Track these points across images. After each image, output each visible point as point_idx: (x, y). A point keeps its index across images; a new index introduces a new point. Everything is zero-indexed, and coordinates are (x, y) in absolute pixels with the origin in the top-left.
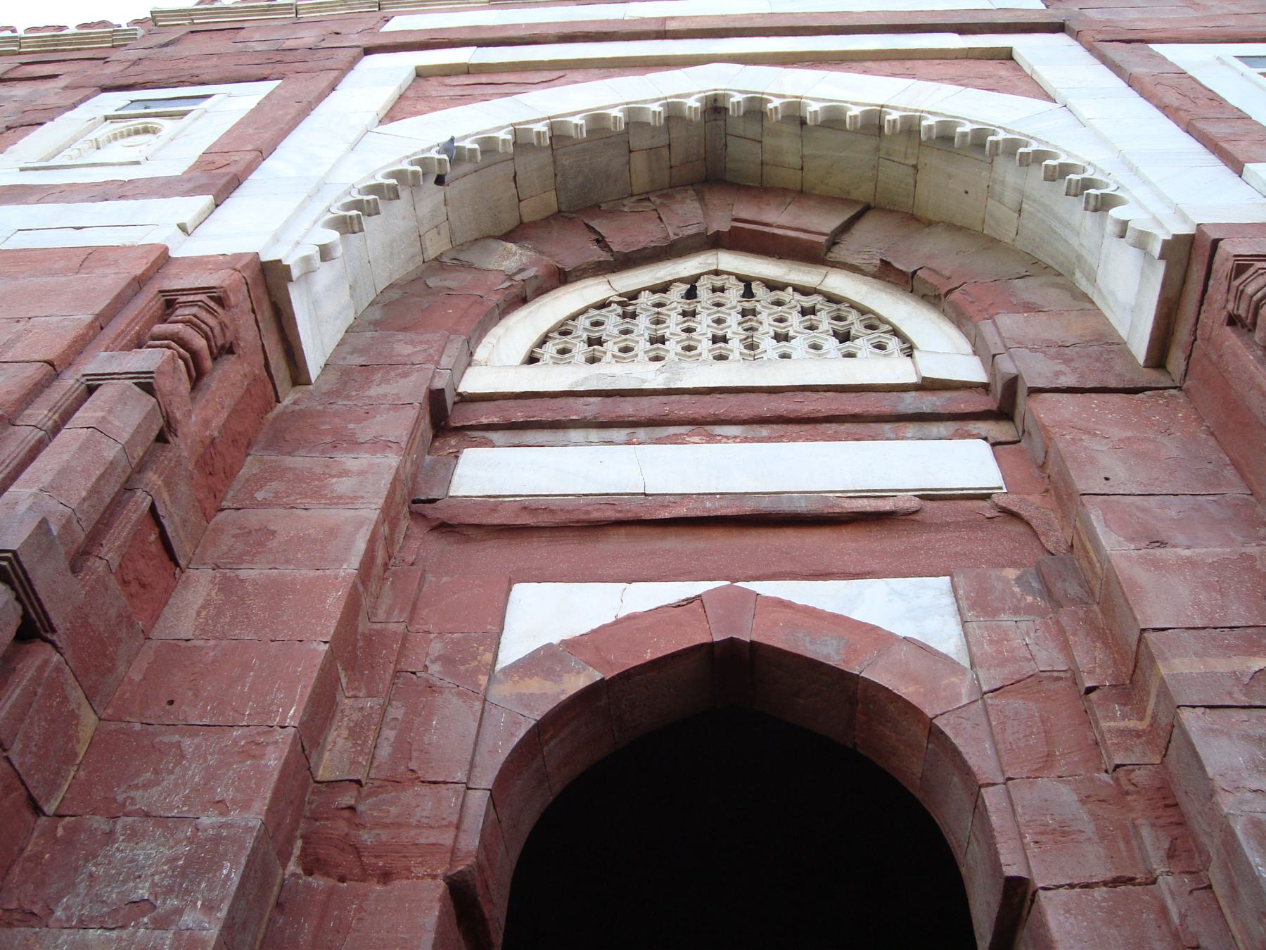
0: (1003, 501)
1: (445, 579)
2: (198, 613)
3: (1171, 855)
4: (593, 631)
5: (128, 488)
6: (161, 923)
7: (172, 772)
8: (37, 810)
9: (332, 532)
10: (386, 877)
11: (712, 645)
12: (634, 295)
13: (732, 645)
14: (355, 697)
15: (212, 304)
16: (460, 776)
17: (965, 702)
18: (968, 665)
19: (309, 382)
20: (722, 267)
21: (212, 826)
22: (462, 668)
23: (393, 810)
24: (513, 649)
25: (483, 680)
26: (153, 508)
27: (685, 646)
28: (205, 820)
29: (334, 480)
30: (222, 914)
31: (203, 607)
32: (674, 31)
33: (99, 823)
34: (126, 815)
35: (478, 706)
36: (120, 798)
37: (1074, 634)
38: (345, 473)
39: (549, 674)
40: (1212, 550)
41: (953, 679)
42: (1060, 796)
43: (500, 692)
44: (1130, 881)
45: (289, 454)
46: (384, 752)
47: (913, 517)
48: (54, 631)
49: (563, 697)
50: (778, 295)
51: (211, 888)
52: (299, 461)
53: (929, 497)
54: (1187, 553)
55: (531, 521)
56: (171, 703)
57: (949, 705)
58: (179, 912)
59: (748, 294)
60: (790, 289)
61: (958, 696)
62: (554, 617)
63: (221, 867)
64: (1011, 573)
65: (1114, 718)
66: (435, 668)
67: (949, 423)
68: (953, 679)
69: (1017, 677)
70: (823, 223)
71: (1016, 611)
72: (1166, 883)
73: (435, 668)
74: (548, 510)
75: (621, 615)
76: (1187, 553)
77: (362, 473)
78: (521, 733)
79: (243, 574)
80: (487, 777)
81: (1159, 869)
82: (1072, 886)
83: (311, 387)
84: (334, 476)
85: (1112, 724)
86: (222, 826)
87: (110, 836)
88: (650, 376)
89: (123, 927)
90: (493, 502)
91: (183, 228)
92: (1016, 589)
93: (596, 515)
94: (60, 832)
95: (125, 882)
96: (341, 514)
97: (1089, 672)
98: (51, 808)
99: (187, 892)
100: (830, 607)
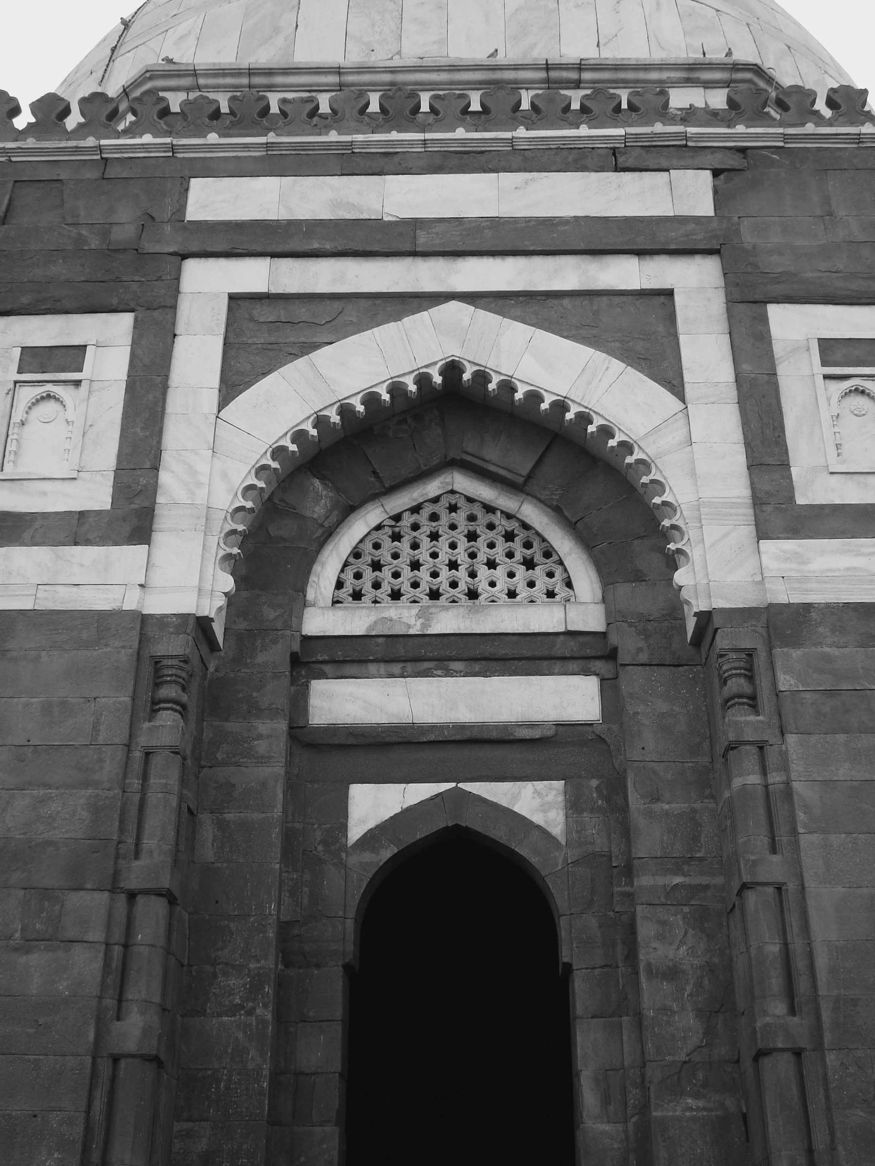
0: (598, 730)
1: (316, 786)
2: (213, 845)
3: (627, 957)
4: (391, 817)
5: (180, 808)
6: (250, 1013)
7: (230, 942)
8: (182, 966)
9: (264, 784)
10: (318, 966)
11: (447, 827)
12: (397, 518)
13: (457, 826)
14: (287, 872)
15: (182, 664)
16: (341, 913)
17: (560, 867)
18: (564, 843)
19: (221, 650)
20: (457, 487)
21: (255, 968)
22: (333, 848)
23: (315, 933)
24: (355, 833)
25: (344, 855)
26: (189, 808)
27: (435, 830)
28: (252, 966)
29: (256, 743)
30: (270, 1009)
31: (214, 841)
32: (421, 252)
33: (208, 968)
34: (218, 964)
35: (343, 871)
36: (213, 956)
37: (615, 833)
38: (260, 737)
39: (375, 850)
40: (678, 807)
41: (557, 854)
42: (592, 922)
43: (353, 860)
44: (610, 966)
45: (227, 720)
46: (306, 901)
47: (553, 739)
48: (176, 899)
49: (381, 864)
50: (491, 518)
51: (263, 997)
52: (232, 726)
53: (559, 725)
54: (667, 807)
55: (354, 742)
56: (217, 902)
57: (551, 869)
58: (254, 1009)
59: (472, 518)
60: (499, 513)
61: (557, 865)
62: (373, 804)
63: (264, 988)
64: (594, 783)
65: (620, 886)
66: (320, 848)
67: (580, 661)
68: (557, 854)
69: (585, 854)
70: (521, 462)
71: (592, 810)
72: (622, 969)
73: (320, 848)
74: (363, 735)
75: (405, 807)
76: (667, 807)
77: (269, 736)
78: (364, 886)
79: (228, 816)
80: (352, 913)
81: (620, 965)
82: (587, 968)
83: (222, 654)
84: (254, 739)
85: (619, 889)
86: (260, 968)
87: (215, 975)
88: (412, 621)
89: (235, 1015)
90: (332, 730)
91: (141, 585)
92: (595, 795)
93: (388, 739)
94: (194, 973)
95: (229, 995)
96: (265, 772)
97: (617, 857)
98: (186, 962)
99: (254, 1000)
100: (504, 803)
